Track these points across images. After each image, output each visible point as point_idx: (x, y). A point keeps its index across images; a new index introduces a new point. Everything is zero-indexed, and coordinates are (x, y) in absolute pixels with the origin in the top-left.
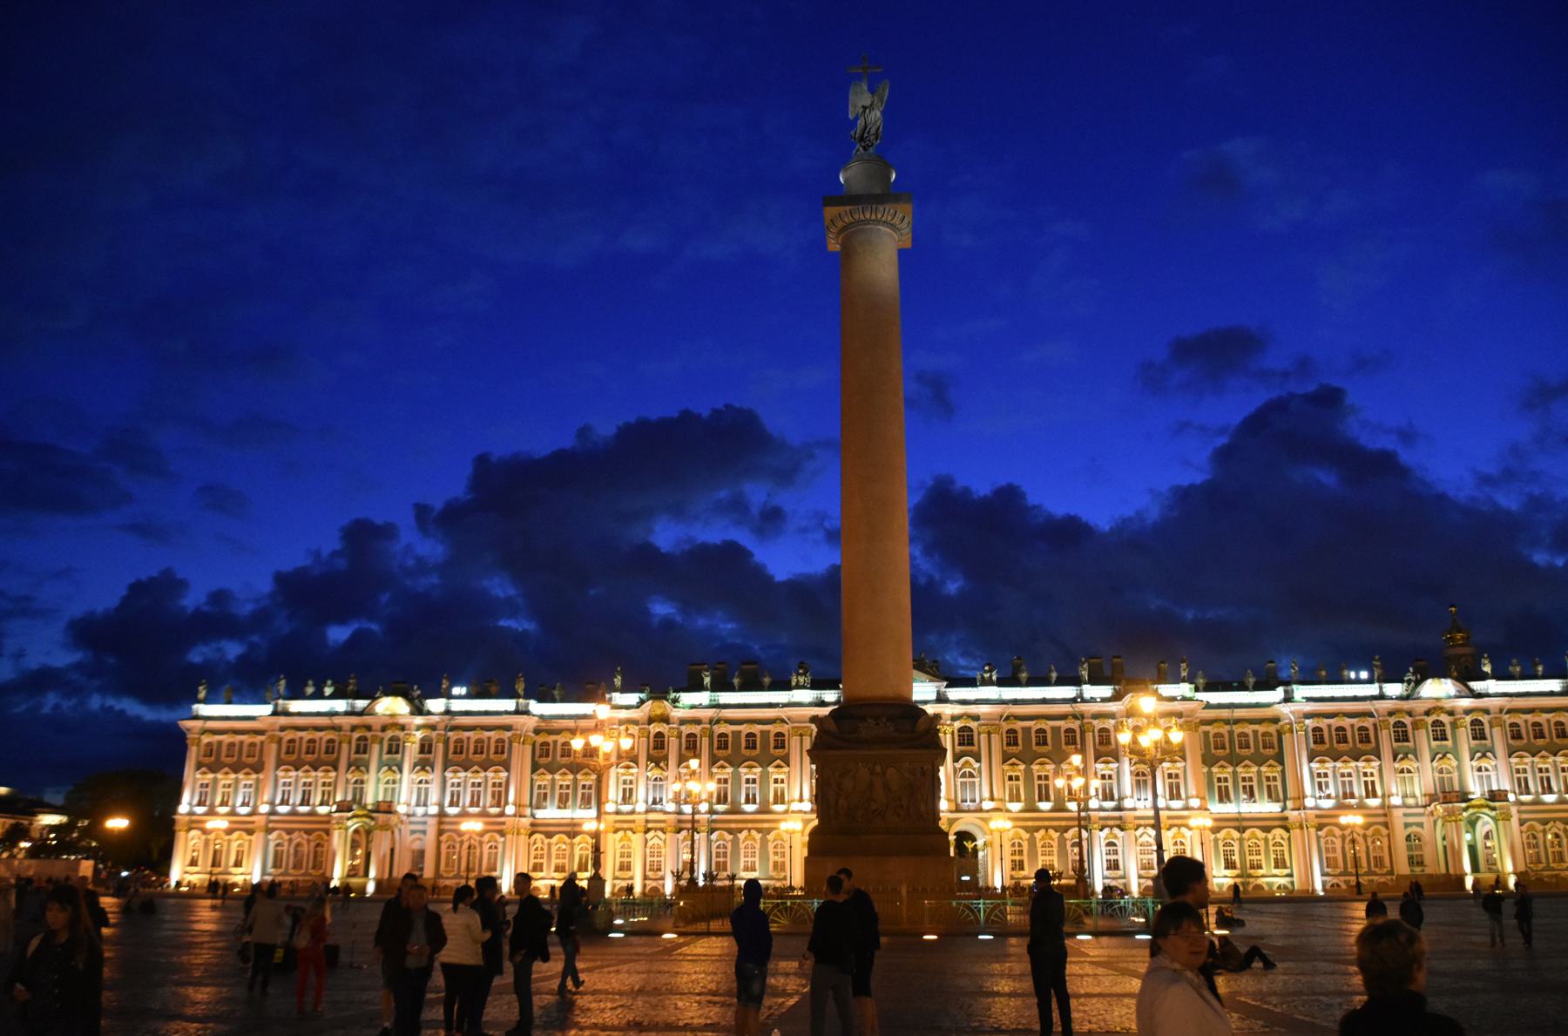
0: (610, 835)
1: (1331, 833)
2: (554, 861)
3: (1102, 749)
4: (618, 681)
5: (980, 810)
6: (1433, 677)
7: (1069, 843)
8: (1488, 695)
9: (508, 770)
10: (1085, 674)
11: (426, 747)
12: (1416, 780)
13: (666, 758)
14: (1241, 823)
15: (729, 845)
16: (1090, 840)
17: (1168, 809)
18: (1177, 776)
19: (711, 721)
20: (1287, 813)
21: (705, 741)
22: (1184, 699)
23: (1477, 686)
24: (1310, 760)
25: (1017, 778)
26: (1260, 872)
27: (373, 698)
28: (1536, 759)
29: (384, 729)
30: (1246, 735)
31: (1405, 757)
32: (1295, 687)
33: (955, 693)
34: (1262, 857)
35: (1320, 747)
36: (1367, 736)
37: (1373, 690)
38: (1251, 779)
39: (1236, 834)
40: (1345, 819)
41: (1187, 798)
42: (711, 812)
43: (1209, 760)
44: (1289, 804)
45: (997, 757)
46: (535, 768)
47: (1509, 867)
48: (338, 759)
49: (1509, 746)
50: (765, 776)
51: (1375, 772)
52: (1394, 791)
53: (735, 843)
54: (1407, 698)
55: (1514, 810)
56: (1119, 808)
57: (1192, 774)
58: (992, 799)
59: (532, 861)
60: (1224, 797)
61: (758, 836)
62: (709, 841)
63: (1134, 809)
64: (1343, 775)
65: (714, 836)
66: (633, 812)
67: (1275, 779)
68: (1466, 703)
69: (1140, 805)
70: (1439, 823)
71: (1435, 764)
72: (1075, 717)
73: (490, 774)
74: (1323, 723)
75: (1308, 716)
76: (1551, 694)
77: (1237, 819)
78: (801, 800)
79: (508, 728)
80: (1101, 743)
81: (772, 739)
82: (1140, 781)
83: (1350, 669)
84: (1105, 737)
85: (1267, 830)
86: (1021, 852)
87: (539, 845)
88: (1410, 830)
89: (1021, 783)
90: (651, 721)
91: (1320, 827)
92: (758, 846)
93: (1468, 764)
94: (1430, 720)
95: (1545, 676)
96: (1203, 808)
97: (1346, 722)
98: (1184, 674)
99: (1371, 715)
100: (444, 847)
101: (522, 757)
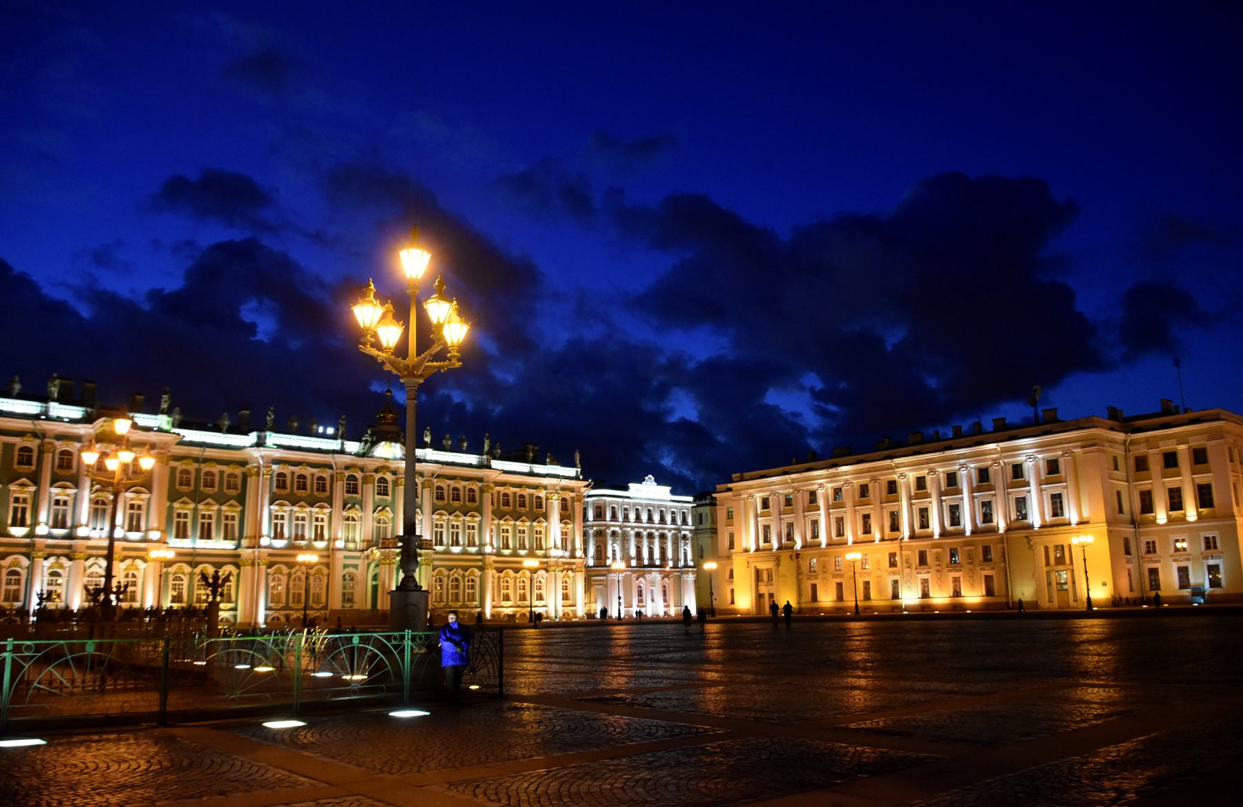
1: (279, 571)
3: (61, 472)
6: (386, 440)
8: (425, 461)
10: (55, 391)
12: (358, 527)
16: (31, 571)
17: (125, 539)
18: (139, 507)
20: (240, 551)
22: (160, 430)
24: (271, 503)
28: (451, 517)
30: (212, 474)
32: (268, 433)
35: (282, 492)
36: (324, 485)
37: (335, 445)
38: (210, 517)
39: (187, 569)
40: (302, 558)
41: (147, 530)
43: (173, 496)
44: (244, 542)
49: (434, 505)
51: (326, 518)
52: (339, 536)
54: (363, 455)
57: (154, 505)
60: (182, 534)
63: (87, 538)
64: (297, 519)
67: (233, 518)
70: (373, 565)
71: (376, 515)
72: (35, 435)
75: (277, 461)
76: (470, 466)
77: (191, 555)
80: (60, 466)
82: (98, 509)
83: (319, 425)
84: (66, 460)
88: (347, 570)
91: (270, 565)
94: (377, 476)
95: (468, 452)
96: (162, 541)
97: (308, 471)
98: (164, 406)
99: (330, 466)
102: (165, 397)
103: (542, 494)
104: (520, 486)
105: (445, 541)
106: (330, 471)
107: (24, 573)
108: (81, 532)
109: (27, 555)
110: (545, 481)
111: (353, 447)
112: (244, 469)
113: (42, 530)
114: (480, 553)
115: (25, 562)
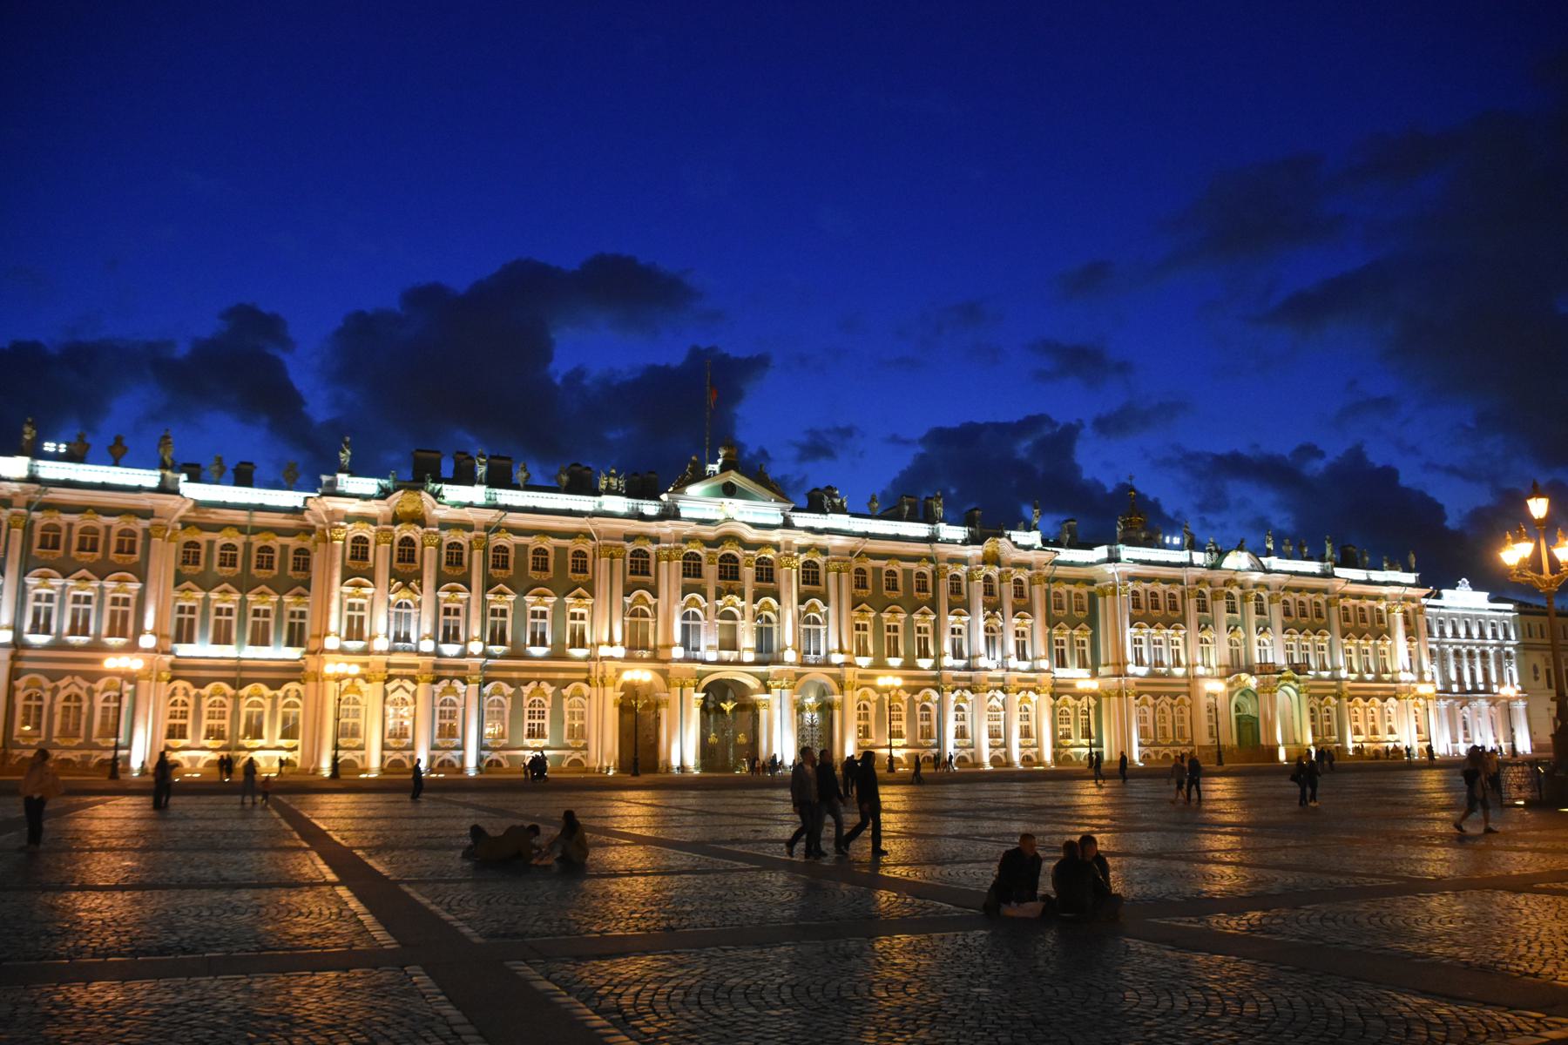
2: (205, 723)
4: (345, 457)
5: (827, 664)
7: (918, 706)
9: (143, 578)
12: (1212, 651)
13: (419, 576)
15: (507, 703)
16: (941, 705)
21: (477, 554)
25: (865, 628)
26: (1070, 742)
33: (801, 519)
34: (1071, 726)
37: (1183, 556)
41: (1034, 659)
42: (486, 655)
44: (1102, 670)
46: (179, 579)
47: (1309, 739)
50: (559, 609)
51: (1181, 641)
53: (517, 699)
58: (841, 651)
61: (549, 689)
63: (986, 669)
65: (487, 690)
68: (1257, 577)
69: (992, 664)
72: (930, 559)
73: (109, 585)
78: (611, 643)
79: (146, 514)
81: (570, 559)
86: (866, 716)
87: (180, 697)
89: (869, 634)
90: (396, 520)
92: (548, 704)
97: (1160, 588)
99: (1181, 582)
100: (20, 697)
101: (164, 560)
103: (1382, 606)
104: (1359, 597)
108: (983, 662)
109: (937, 689)
110: (1385, 590)
111: (1199, 557)
112: (1093, 589)
113: (948, 661)
114: (1332, 678)
115: (935, 695)
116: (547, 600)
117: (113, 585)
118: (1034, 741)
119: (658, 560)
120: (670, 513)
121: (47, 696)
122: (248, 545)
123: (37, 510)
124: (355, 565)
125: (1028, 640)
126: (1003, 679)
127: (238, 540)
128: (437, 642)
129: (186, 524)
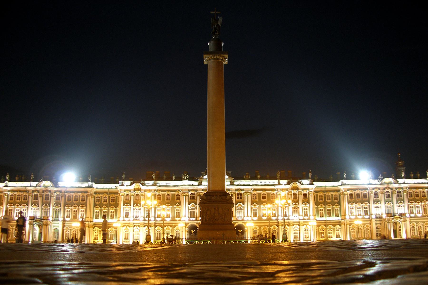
0: (122, 228)
4: (124, 176)
11: (58, 198)
14: (326, 223)
16: (278, 229)
19: (155, 190)
23: (400, 181)
27: (40, 182)
28: (416, 203)
29: (44, 191)
31: (377, 203)
33: (236, 182)
39: (324, 227)
41: (310, 216)
43: (317, 203)
45: (249, 203)
48: (28, 202)
49: (408, 199)
55: (408, 219)
56: (288, 219)
59: (94, 236)
61: (171, 228)
62: (155, 230)
64: (358, 208)
65: (156, 228)
66: (129, 221)
67: (337, 210)
71: (386, 205)
74: (353, 192)
75: (348, 190)
77: (325, 222)
85: (334, 226)
87: (97, 231)
88: (377, 225)
90: (135, 190)
91: (350, 225)
93: (395, 205)
99: (367, 189)
100: (65, 231)
101: (91, 202)
102: (310, 173)
105: (414, 213)
106: (368, 191)
107: (277, 230)
116: (170, 207)
117: (81, 208)
118: (309, 239)
119: (197, 196)
120: (200, 184)
121: (69, 231)
122: (109, 197)
123: (66, 192)
124: (126, 201)
125: (308, 210)
126: (299, 222)
127: (107, 196)
128: (144, 217)
129: (96, 193)
